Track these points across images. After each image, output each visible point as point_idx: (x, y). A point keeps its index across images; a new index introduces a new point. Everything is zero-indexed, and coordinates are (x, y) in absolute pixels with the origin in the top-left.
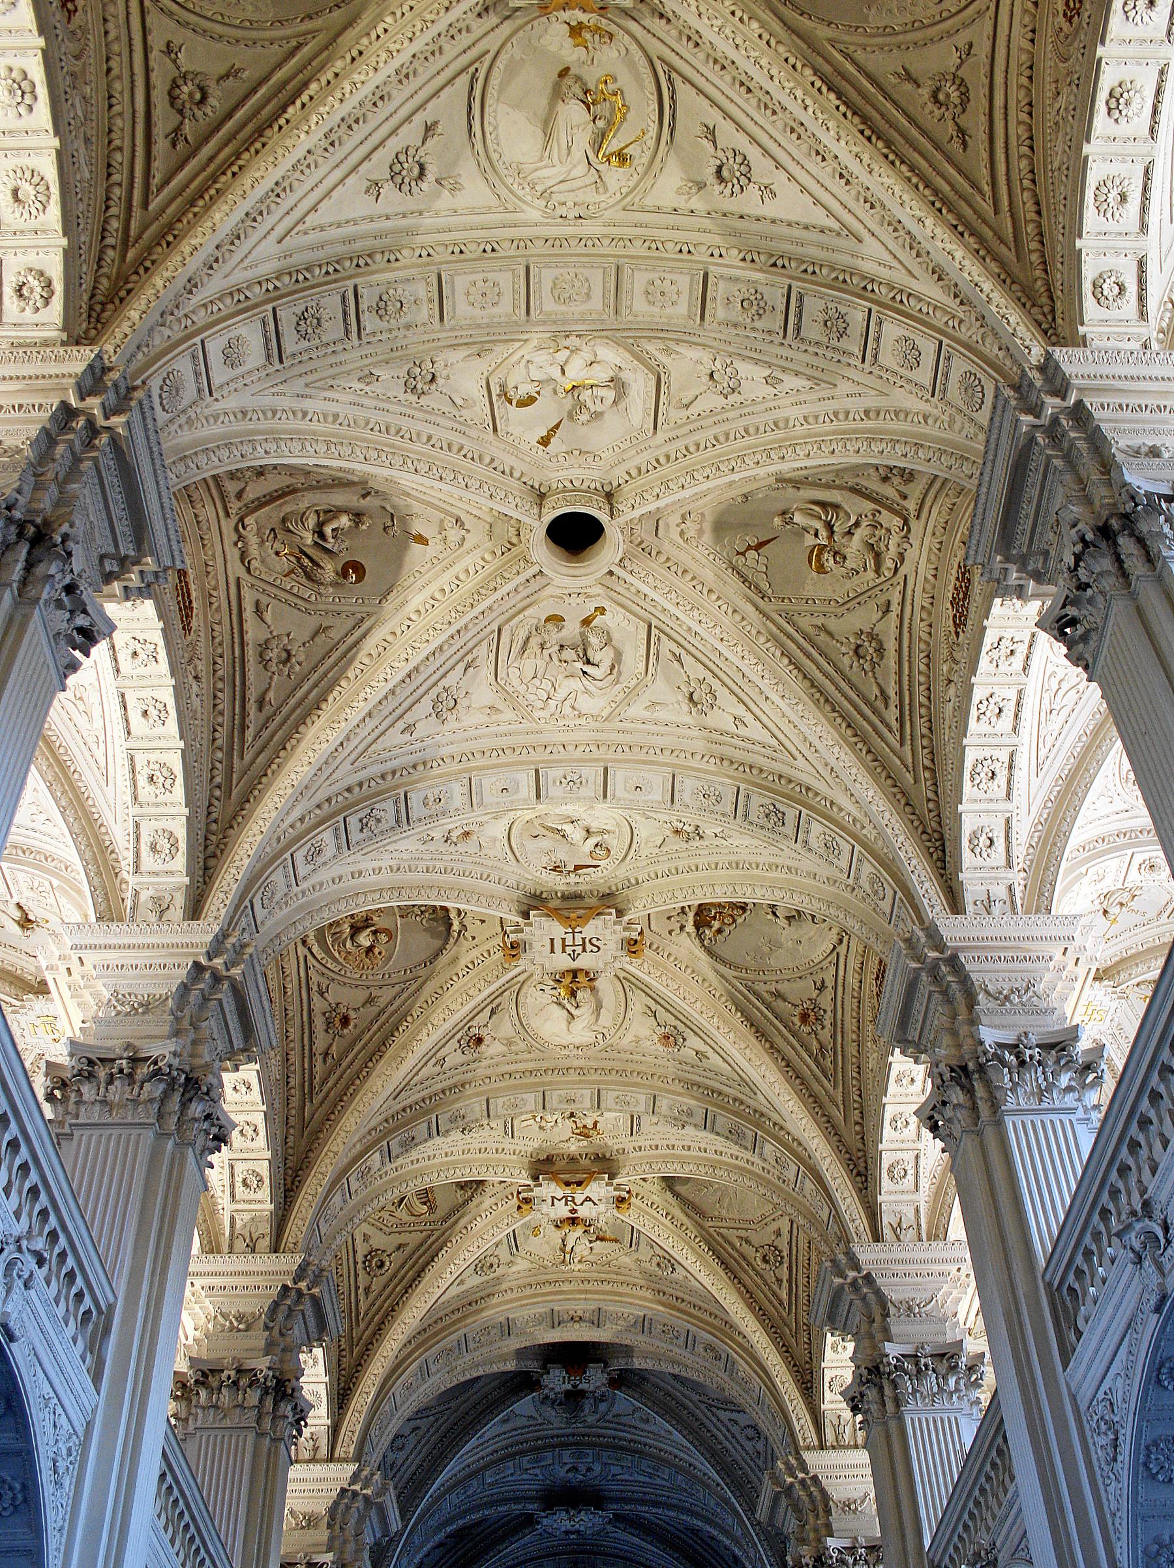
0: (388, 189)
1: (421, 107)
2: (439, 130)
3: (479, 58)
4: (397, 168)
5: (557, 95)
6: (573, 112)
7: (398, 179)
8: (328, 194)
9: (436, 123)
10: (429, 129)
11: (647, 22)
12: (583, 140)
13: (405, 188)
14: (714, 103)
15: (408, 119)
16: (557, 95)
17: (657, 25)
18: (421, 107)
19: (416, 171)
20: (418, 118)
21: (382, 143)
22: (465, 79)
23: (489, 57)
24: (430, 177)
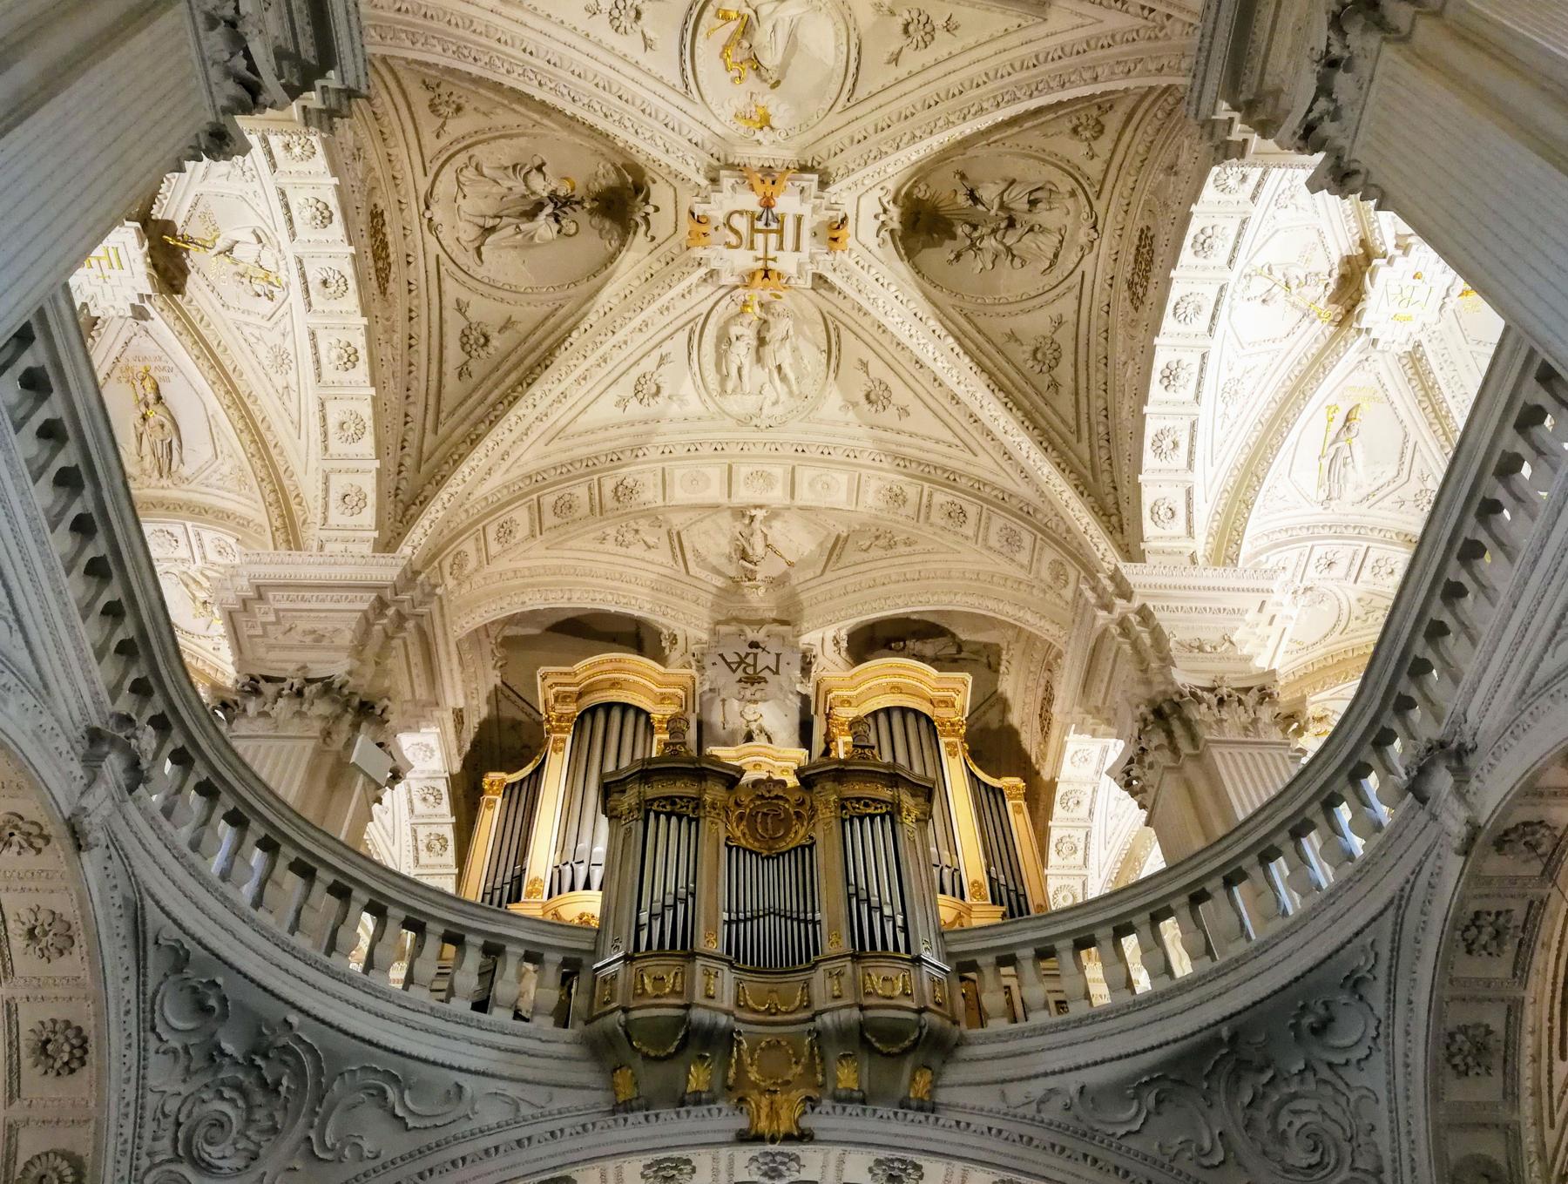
0: (939, 22)
1: (899, 82)
2: (886, 57)
3: (846, 109)
4: (928, 38)
5: (784, 67)
6: (770, 59)
7: (928, 28)
8: (992, 40)
9: (889, 62)
10: (895, 59)
11: (707, 133)
12: (762, 35)
13: (923, 19)
14: (648, 73)
15: (911, 75)
16: (784, 67)
17: (699, 134)
18: (899, 82)
19: (911, 28)
20: (901, 71)
21: (937, 63)
22: (861, 93)
23: (838, 107)
24: (899, 22)
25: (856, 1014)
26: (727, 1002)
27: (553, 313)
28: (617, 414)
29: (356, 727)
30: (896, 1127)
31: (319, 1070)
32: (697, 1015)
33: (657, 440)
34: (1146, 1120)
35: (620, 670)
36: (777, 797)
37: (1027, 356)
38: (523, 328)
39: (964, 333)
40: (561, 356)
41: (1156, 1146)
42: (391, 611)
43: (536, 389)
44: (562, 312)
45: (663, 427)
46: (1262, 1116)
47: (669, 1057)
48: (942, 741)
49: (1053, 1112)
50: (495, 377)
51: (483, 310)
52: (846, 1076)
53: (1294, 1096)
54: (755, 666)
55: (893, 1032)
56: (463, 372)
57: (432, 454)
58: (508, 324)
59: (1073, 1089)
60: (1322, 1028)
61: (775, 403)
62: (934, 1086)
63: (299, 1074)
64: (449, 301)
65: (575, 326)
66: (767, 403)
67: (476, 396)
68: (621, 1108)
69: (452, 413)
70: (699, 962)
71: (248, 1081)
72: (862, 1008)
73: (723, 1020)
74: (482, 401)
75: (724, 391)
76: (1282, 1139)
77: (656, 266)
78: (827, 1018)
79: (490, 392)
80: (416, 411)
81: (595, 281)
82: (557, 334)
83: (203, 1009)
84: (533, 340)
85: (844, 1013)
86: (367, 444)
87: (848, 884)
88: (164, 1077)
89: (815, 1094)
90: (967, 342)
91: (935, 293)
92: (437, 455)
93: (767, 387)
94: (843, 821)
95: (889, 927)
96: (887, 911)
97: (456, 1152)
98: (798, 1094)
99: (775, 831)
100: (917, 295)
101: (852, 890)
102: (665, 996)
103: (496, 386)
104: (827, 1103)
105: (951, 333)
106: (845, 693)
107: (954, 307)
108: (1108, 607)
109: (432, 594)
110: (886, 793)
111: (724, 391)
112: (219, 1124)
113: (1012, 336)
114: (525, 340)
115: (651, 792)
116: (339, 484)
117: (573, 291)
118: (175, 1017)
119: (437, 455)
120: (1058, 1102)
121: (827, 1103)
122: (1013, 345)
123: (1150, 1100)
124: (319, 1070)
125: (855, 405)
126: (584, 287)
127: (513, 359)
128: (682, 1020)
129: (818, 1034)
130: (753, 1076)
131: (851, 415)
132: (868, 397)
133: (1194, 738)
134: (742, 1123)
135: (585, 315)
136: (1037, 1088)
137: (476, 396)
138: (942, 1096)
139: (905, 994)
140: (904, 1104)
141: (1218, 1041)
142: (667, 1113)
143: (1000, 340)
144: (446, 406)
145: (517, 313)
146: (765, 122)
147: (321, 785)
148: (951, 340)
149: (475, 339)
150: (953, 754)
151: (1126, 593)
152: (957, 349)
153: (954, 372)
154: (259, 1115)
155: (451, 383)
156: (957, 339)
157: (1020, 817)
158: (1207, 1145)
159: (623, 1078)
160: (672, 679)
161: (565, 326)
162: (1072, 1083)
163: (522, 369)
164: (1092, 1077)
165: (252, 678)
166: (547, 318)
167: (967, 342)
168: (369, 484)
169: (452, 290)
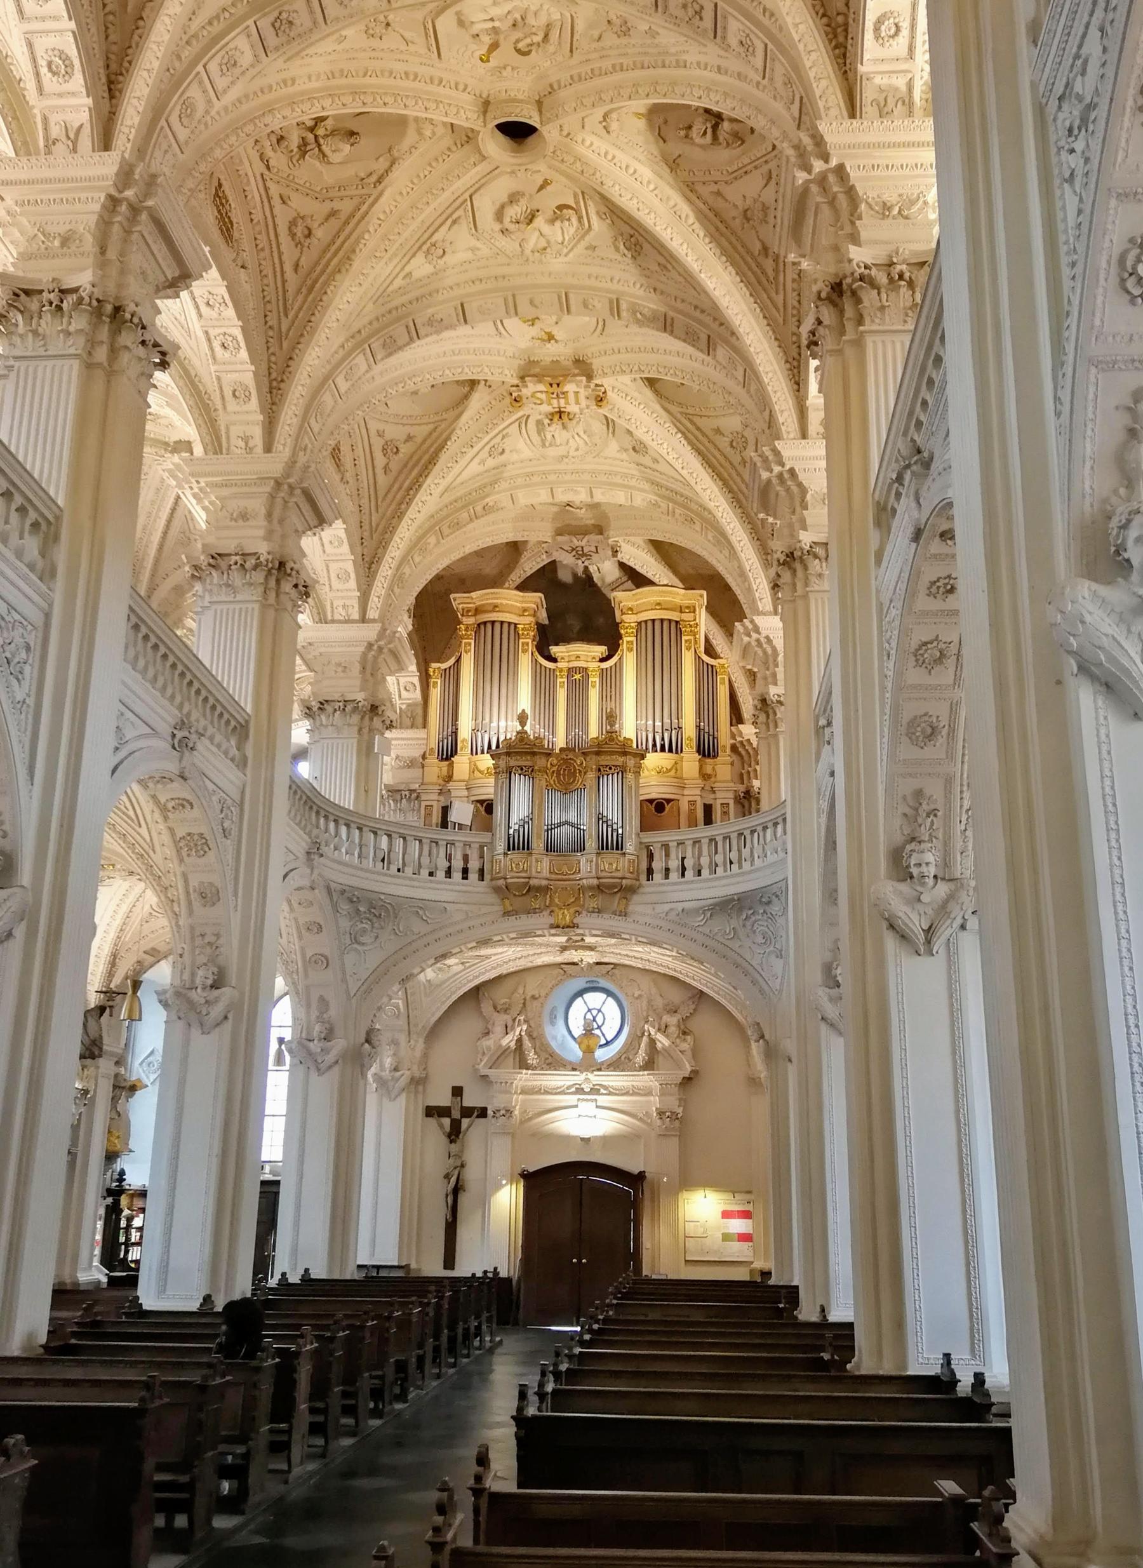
25: (595, 882)
26: (545, 873)
27: (435, 429)
28: (481, 468)
29: (371, 719)
30: (611, 923)
31: (394, 909)
32: (533, 882)
33: (505, 475)
37: (727, 444)
38: (419, 440)
39: (687, 429)
40: (444, 457)
42: (375, 647)
43: (429, 481)
44: (439, 430)
45: (509, 467)
46: (748, 923)
47: (523, 895)
48: (684, 638)
49: (672, 916)
50: (406, 471)
51: (395, 432)
52: (593, 904)
53: (756, 921)
55: (611, 886)
56: (386, 469)
57: (378, 526)
58: (409, 438)
59: (680, 909)
60: (769, 903)
61: (577, 449)
62: (627, 905)
63: (387, 910)
64: (373, 433)
65: (448, 438)
66: (573, 449)
67: (395, 488)
68: (507, 914)
69: (384, 499)
70: (534, 857)
71: (371, 917)
72: (598, 878)
73: (544, 883)
74: (400, 488)
75: (544, 445)
76: (754, 932)
77: (493, 402)
78: (584, 881)
79: (404, 481)
80: (365, 501)
81: (457, 411)
82: (439, 441)
83: (352, 902)
84: (425, 446)
85: (591, 881)
86: (346, 548)
88: (345, 924)
90: (690, 435)
91: (670, 406)
92: (381, 527)
93: (571, 441)
95: (615, 834)
96: (615, 827)
97: (449, 930)
98: (572, 910)
100: (658, 407)
103: (406, 478)
104: (584, 913)
105: (680, 431)
106: (630, 604)
107: (681, 413)
108: (749, 635)
109: (394, 636)
110: (621, 759)
111: (544, 445)
112: (364, 931)
113: (718, 431)
114: (419, 447)
115: (513, 763)
116: (334, 567)
117: (445, 416)
118: (345, 907)
119: (381, 527)
120: (674, 913)
121: (584, 913)
122: (718, 437)
123: (708, 915)
124: (394, 909)
125: (626, 450)
126: (451, 415)
127: (415, 458)
129: (582, 889)
130: (556, 900)
131: (624, 456)
132: (634, 449)
133: (776, 726)
134: (551, 920)
135: (454, 430)
136: (667, 907)
137: (396, 486)
138: (631, 908)
139: (617, 870)
141: (733, 900)
142: (524, 917)
143: (710, 433)
144: (381, 494)
145: (414, 430)
146: (551, 337)
147: (364, 758)
148: (679, 435)
149: (392, 449)
150: (688, 649)
151: (757, 630)
152: (684, 442)
153: (680, 461)
154: (376, 925)
155: (382, 479)
156: (683, 433)
157: (722, 687)
159: (507, 902)
161: (444, 436)
162: (680, 906)
163: (421, 464)
164: (687, 905)
165: (321, 703)
166: (431, 434)
167: (690, 435)
168: (350, 567)
169: (374, 426)
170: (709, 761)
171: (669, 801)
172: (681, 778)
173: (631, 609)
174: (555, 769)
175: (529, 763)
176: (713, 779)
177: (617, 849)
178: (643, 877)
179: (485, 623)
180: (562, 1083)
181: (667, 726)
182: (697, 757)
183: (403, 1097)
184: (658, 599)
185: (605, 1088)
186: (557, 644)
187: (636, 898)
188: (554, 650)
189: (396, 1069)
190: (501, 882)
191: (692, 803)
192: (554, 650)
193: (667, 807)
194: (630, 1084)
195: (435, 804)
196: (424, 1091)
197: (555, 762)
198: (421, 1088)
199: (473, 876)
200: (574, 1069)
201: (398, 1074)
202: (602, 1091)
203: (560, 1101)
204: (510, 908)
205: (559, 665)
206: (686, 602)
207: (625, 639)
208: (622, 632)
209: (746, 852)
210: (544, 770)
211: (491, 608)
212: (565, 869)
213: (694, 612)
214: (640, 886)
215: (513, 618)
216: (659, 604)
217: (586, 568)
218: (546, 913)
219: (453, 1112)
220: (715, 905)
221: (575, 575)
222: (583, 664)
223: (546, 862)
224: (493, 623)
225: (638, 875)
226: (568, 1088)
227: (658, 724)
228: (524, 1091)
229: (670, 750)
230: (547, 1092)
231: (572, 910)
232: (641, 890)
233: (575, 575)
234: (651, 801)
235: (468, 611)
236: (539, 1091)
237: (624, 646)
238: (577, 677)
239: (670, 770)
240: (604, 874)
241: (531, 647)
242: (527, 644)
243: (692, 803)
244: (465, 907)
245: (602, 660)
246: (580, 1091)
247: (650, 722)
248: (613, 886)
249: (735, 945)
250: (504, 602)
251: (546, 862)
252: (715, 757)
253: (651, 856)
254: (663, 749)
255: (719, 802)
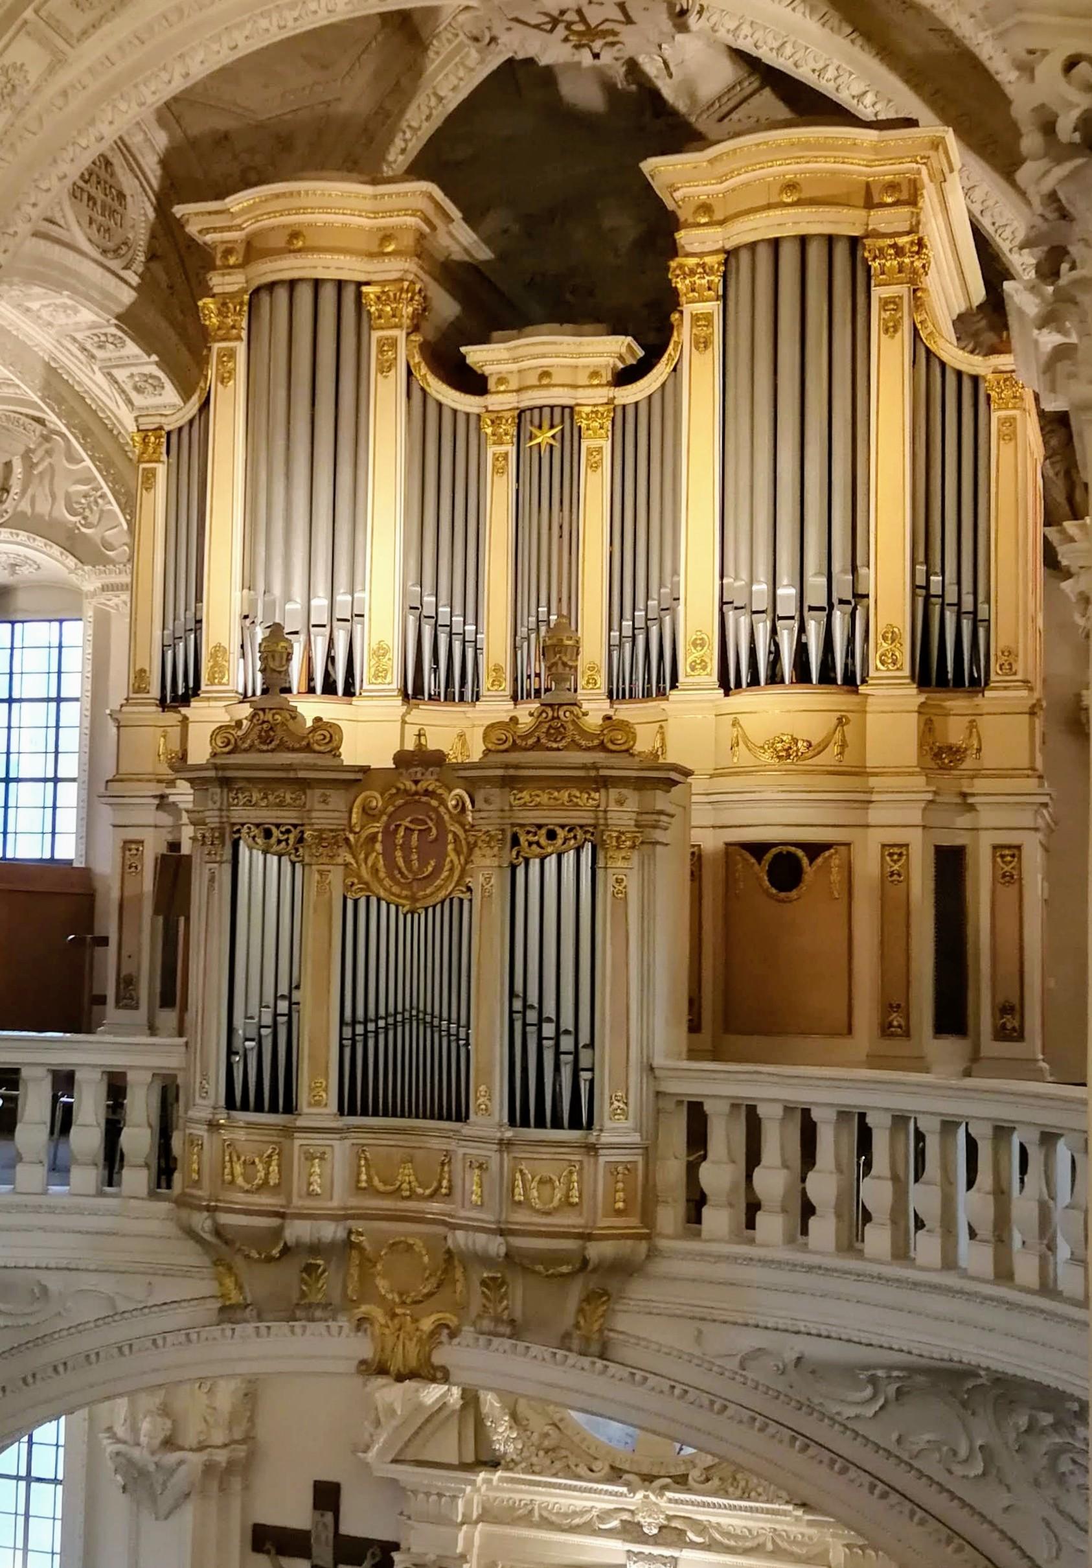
25: (496, 1246)
34: (882, 1408)
35: (298, 211)
36: (427, 793)
41: (894, 1436)
54: (583, 19)
59: (790, 1356)
68: (229, 1313)
73: (330, 1231)
85: (481, 1239)
87: (512, 994)
89: (453, 1321)
94: (514, 868)
99: (423, 863)
101: (518, 1005)
102: (259, 1189)
106: (702, 191)
123: (891, 1390)
128: (278, 1232)
130: (382, 1284)
139: (567, 1203)
140: (564, 1341)
158: (963, 1452)
160: (387, 203)
164: (817, 1350)
170: (957, 703)
171: (814, 850)
172: (860, 772)
173: (706, 208)
174: (377, 827)
175: (288, 816)
176: (968, 763)
177: (575, 1124)
178: (670, 1216)
179: (271, 286)
180: (589, 1504)
181: (816, 595)
182: (912, 696)
183: (188, 1514)
184: (790, 170)
185: (701, 1528)
186: (484, 340)
187: (639, 1291)
188: (476, 355)
189: (169, 1443)
190: (201, 1222)
191: (895, 851)
192: (476, 355)
193: (809, 870)
194: (768, 1525)
195: (148, 836)
196: (246, 1488)
197: (377, 802)
198: (236, 1484)
199: (135, 1178)
200: (616, 1474)
201: (173, 1457)
202: (691, 1536)
203: (581, 1548)
204: (235, 1297)
205: (494, 401)
206: (886, 171)
207: (689, 309)
208: (681, 285)
209: (1024, 1207)
210: (333, 840)
211: (280, 241)
212: (406, 1176)
213: (913, 202)
214: (653, 1253)
215: (349, 268)
216: (791, 186)
217: (632, 66)
218: (344, 1322)
219: (315, 1550)
220: (912, 1370)
221: (609, 87)
222: (559, 396)
223: (340, 1150)
224: (292, 284)
225: (648, 1217)
226: (605, 1515)
227: (786, 591)
228: (487, 1515)
229: (827, 677)
230: (547, 1523)
231: (427, 1324)
232: (661, 1267)
233: (609, 87)
234: (757, 849)
235: (228, 252)
236: (526, 1518)
237: (684, 334)
238: (544, 437)
239: (824, 746)
240: (522, 1217)
241: (405, 350)
242: (394, 343)
243: (895, 851)
244: (107, 1285)
245: (626, 376)
246: (631, 1531)
247: (761, 587)
248: (554, 1258)
249: (993, 1501)
250: (320, 218)
251: (340, 1150)
252: (978, 685)
253: (697, 1138)
254: (802, 674)
255: (986, 841)
